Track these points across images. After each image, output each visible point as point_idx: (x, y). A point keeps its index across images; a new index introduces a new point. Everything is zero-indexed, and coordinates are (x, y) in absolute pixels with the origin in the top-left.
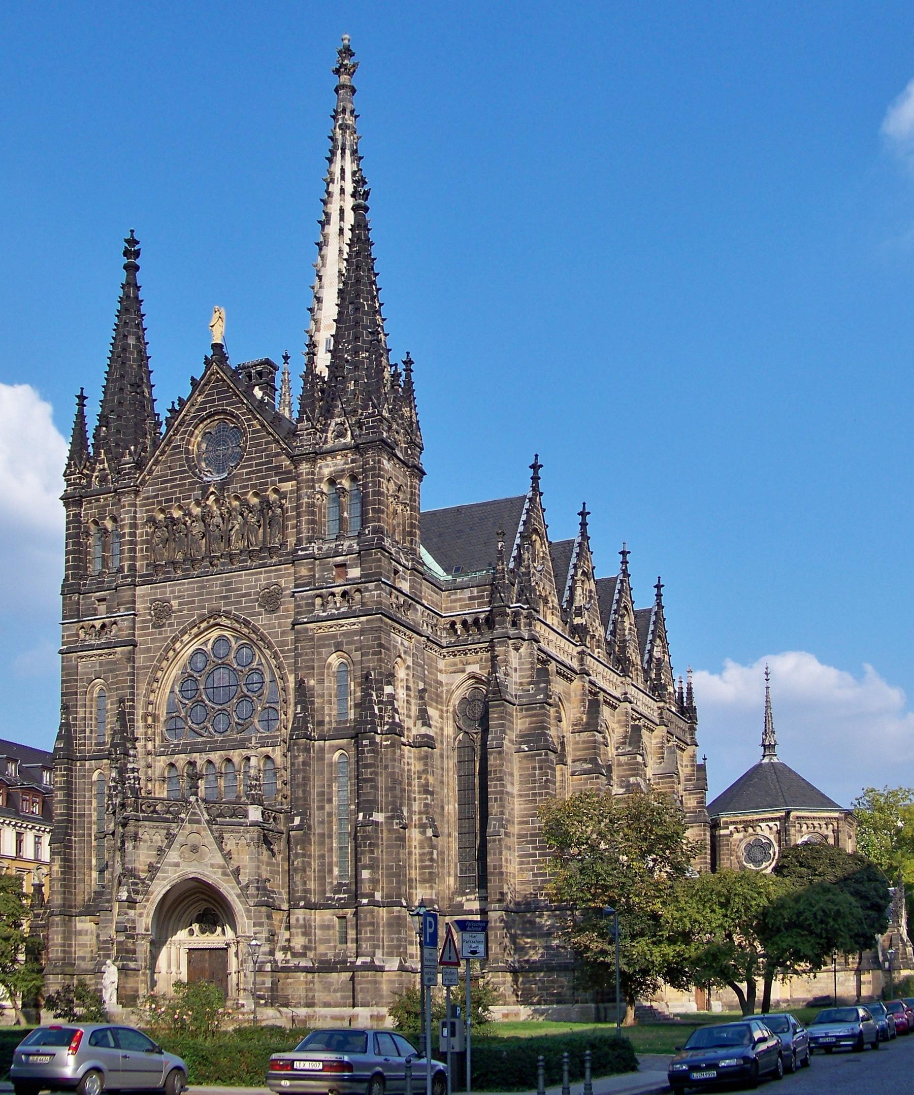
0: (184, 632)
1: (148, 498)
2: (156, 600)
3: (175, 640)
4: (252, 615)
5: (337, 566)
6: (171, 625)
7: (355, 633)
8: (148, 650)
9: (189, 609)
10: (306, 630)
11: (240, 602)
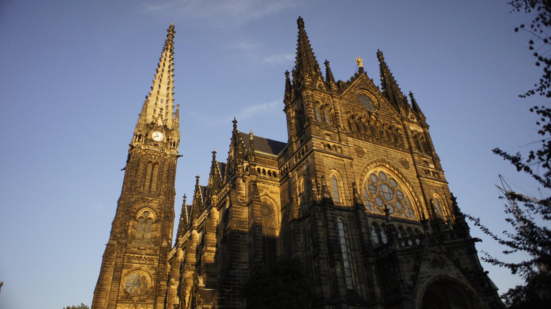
0: (372, 163)
2: (356, 145)
3: (368, 165)
4: (399, 167)
5: (425, 161)
6: (365, 158)
7: (439, 188)
8: (357, 165)
9: (372, 155)
10: (424, 180)
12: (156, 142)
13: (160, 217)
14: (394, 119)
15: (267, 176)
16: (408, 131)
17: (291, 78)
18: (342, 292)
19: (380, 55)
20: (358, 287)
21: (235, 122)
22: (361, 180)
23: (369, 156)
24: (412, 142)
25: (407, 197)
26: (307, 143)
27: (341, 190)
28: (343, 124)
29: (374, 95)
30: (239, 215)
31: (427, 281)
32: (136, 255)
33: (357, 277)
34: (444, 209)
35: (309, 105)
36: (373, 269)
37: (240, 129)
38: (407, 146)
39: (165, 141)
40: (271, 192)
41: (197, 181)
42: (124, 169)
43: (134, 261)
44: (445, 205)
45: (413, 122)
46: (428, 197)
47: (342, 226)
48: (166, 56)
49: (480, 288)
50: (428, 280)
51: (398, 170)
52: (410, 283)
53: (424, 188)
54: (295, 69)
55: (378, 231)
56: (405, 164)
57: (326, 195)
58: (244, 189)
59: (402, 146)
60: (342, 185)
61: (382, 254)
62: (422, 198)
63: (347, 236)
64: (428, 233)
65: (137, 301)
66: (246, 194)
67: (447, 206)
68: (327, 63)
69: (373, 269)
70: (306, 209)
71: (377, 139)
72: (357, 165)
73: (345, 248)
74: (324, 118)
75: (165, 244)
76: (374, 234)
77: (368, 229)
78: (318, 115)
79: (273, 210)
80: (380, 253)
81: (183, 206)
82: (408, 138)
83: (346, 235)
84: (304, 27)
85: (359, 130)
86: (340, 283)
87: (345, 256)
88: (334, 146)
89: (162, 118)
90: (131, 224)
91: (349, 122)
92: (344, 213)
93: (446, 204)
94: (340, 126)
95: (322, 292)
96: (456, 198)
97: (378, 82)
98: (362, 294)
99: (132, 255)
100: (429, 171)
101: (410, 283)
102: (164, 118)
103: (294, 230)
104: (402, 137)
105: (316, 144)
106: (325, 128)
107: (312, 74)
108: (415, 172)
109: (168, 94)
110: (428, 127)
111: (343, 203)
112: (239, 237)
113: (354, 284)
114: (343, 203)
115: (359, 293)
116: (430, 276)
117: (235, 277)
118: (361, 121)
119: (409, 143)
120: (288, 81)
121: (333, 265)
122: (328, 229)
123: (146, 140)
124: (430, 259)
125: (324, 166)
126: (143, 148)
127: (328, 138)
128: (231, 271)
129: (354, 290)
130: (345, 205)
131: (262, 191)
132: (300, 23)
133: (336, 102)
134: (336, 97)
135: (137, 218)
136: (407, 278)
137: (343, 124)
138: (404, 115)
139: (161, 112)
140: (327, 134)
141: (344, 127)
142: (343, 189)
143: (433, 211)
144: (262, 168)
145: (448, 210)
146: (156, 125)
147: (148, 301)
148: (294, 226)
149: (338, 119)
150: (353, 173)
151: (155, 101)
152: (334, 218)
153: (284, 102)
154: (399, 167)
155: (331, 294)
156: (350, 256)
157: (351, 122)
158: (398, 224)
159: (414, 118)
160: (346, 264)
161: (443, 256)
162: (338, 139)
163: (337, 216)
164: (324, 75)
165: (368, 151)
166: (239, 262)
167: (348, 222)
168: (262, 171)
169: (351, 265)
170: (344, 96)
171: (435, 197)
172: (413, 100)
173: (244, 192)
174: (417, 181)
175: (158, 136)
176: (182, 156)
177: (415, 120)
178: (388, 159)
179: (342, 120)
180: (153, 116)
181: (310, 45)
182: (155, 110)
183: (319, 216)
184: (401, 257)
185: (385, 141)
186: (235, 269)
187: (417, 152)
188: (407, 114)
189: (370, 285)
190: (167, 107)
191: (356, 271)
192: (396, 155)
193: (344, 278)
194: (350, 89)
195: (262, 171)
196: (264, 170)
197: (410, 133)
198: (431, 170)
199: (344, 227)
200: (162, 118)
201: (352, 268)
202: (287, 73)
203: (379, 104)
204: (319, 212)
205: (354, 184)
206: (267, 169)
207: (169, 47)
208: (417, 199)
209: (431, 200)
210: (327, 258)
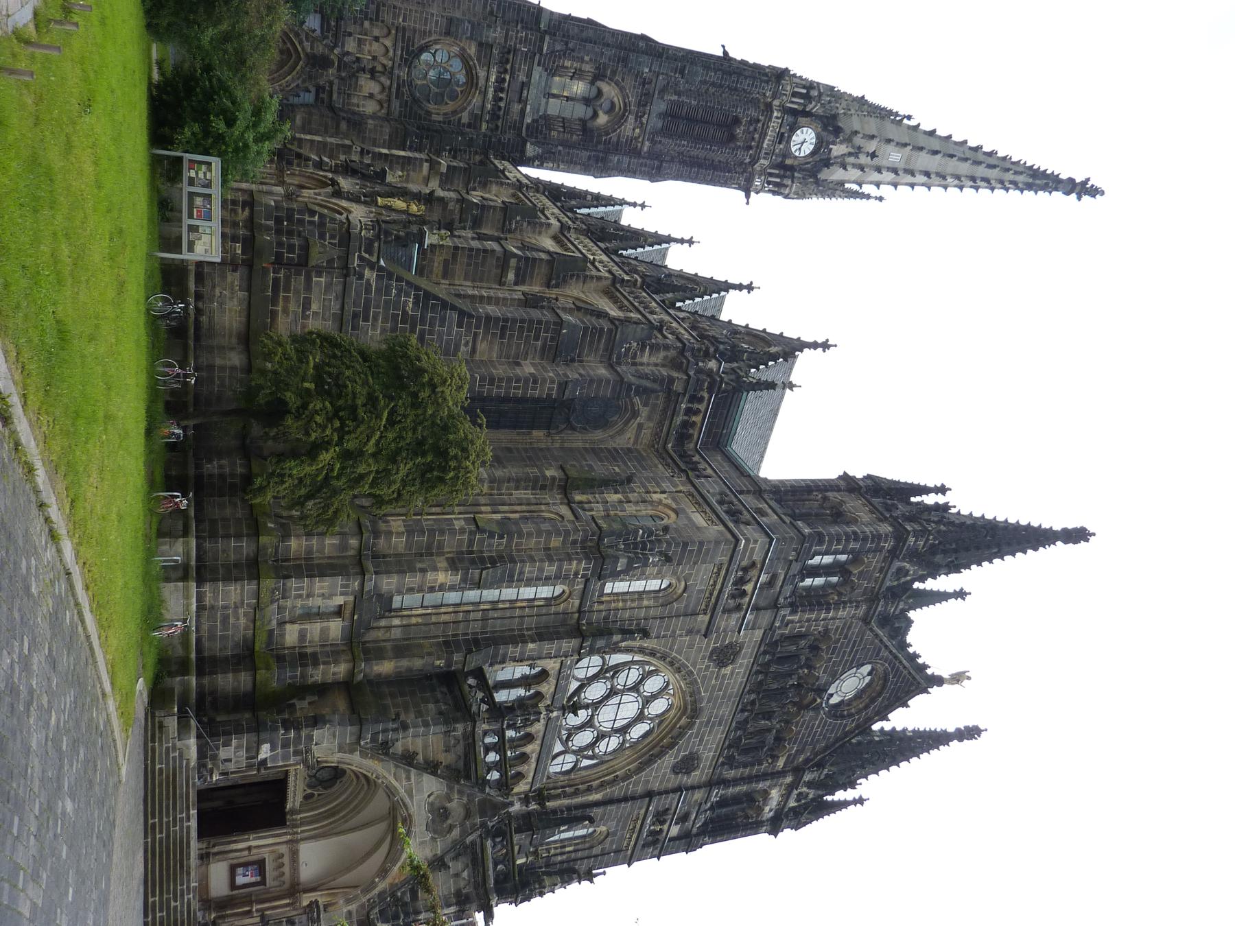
1: (850, 628)
4: (679, 751)
6: (708, 667)
8: (691, 646)
9: (714, 687)
10: (640, 808)
11: (696, 737)
12: (790, 137)
13: (599, 142)
14: (799, 752)
15: (679, 420)
16: (768, 783)
17: (930, 499)
18: (388, 583)
19: (970, 733)
20: (396, 622)
21: (825, 346)
22: (652, 653)
23: (711, 679)
24: (738, 789)
25: (602, 763)
26: (756, 526)
27: (632, 601)
28: (797, 620)
29: (867, 707)
30: (591, 342)
31: (401, 788)
32: (508, 77)
33: (420, 620)
34: (567, 849)
35: (855, 540)
36: (438, 662)
37: (805, 358)
38: (730, 774)
39: (788, 162)
40: (640, 426)
41: (682, 241)
42: (725, 53)
43: (494, 70)
44: (575, 851)
45: (786, 797)
46: (596, 812)
47: (544, 596)
48: (1016, 173)
49: (376, 910)
50: (402, 791)
51: (671, 746)
52: (399, 748)
53: (623, 805)
54: (953, 511)
55: (525, 682)
56: (687, 765)
57: (622, 564)
58: (653, 360)
59: (730, 762)
60: (645, 603)
61: (470, 686)
62: (596, 797)
63: (519, 604)
64: (512, 804)
65: (399, 77)
66: (642, 364)
67: (573, 855)
68: (961, 594)
69: (438, 662)
70: (592, 510)
71: (753, 703)
72: (691, 646)
73: (490, 599)
74: (820, 576)
75: (530, 150)
76: (521, 670)
77: (532, 659)
78: (828, 559)
79: (596, 428)
80: (471, 681)
81: (622, 202)
82: (750, 779)
83: (524, 604)
84: (1065, 543)
85: (781, 660)
86: (411, 580)
87: (472, 595)
88: (744, 593)
89: (850, 154)
90: (587, 67)
91: (801, 636)
92: (577, 603)
93: (580, 854)
94: (793, 612)
95: (390, 533)
96: (592, 882)
97: (900, 720)
98: (379, 628)
99: (508, 67)
100: (662, 823)
101: (399, 748)
102: (852, 160)
103: (545, 477)
104: (753, 765)
105: (753, 549)
106: (791, 573)
107: (934, 554)
108: (663, 788)
109: (913, 175)
110: (774, 831)
111: (602, 602)
112: (536, 339)
113: (405, 613)
114: (602, 602)
115: (383, 623)
116: (411, 796)
117: (442, 324)
118: (801, 667)
119: (735, 782)
120: (925, 490)
121: (453, 565)
122: (542, 561)
123: (794, 113)
124: (450, 800)
125: (695, 563)
126: (776, 102)
127: (764, 578)
128: (455, 315)
129: (390, 610)
130: (596, 606)
131: (645, 405)
132: (1077, 535)
133: (857, 607)
134: (869, 609)
135: (599, 83)
136: (410, 739)
137: (797, 620)
138: (808, 777)
140: (774, 577)
141: (792, 622)
142: (635, 604)
143: (564, 822)
144: (702, 407)
145: (564, 857)
146: (831, 138)
147: (396, 104)
148: (553, 478)
149: (812, 611)
150: (674, 632)
151: (897, 139)
152: (567, 577)
153: (869, 477)
154: (679, 751)
155: (384, 556)
156: (471, 608)
157: (803, 643)
158: (538, 732)
159: (798, 800)
160: (453, 597)
161: (456, 833)
162: (762, 603)
163: (571, 585)
164: (930, 585)
165: (724, 675)
166: (476, 335)
167: (553, 609)
168: (696, 406)
169: (451, 609)
170: (871, 630)
171: (598, 830)
172: (844, 804)
173: (645, 359)
174: (640, 789)
175: (804, 141)
177: (792, 803)
178: (701, 723)
179: (808, 620)
180: (856, 132)
181: (1014, 555)
182: (873, 137)
183: (574, 542)
184: (459, 733)
185: (746, 721)
186: (460, 325)
187: (713, 799)
188: (810, 785)
189: (401, 650)
190: (879, 170)
191: (434, 619)
192: (708, 744)
193: (420, 590)
194: (886, 647)
195: (696, 406)
196: (697, 412)
197: (761, 785)
198: (666, 827)
199: (540, 599)
200: (850, 154)
201: (443, 610)
202: (942, 490)
203: (843, 717)
204: (583, 541)
205: (645, 634)
206: (697, 419)
207: (1038, 182)
208: (595, 784)
209: (591, 820)
210: (472, 552)
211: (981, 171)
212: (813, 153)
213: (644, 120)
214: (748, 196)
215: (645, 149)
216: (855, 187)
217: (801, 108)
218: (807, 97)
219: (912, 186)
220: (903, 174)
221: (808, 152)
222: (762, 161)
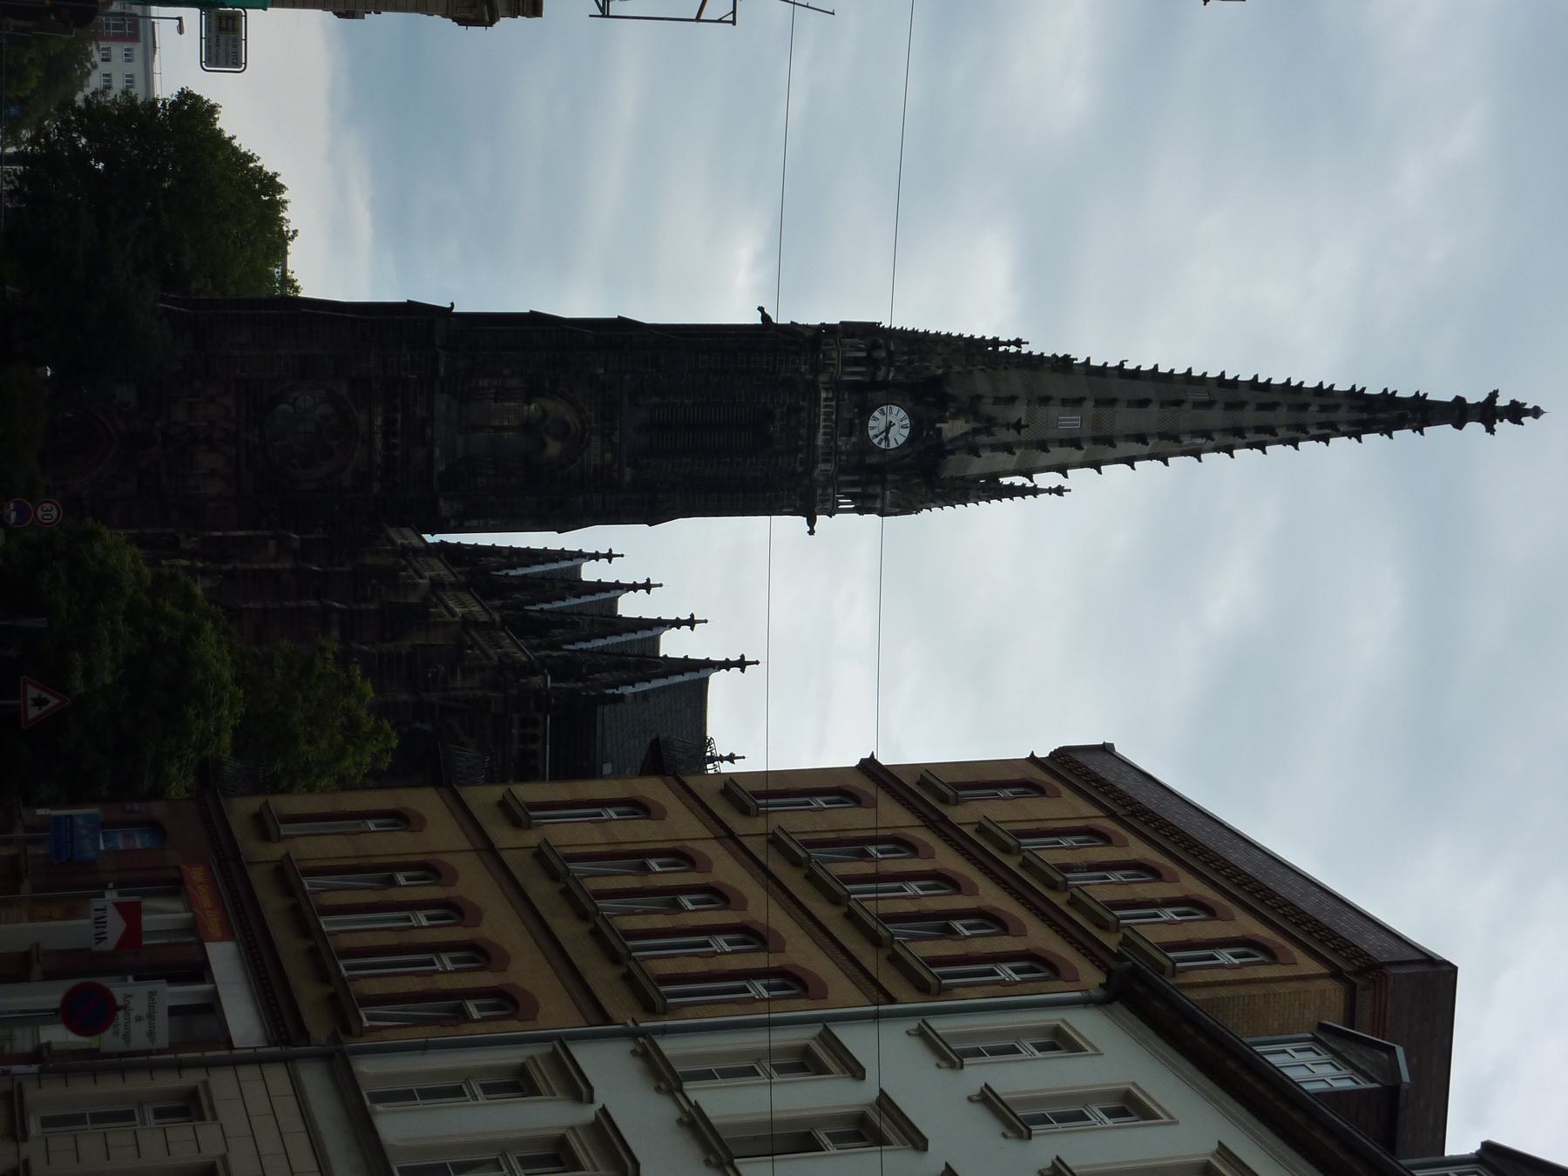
21: (742, 664)
32: (399, 416)
39: (872, 460)
42: (765, 317)
81: (581, 555)
102: (983, 439)
109: (1113, 445)
123: (855, 387)
126: (823, 378)
139: (1008, 426)
176: (812, 532)
182: (1012, 400)
200: (976, 432)
211: (1249, 416)
212: (910, 441)
213: (616, 439)
214: (811, 522)
215: (628, 478)
216: (1018, 481)
217: (867, 379)
218: (871, 362)
219: (1130, 462)
220: (1099, 448)
221: (901, 440)
222: (822, 466)
